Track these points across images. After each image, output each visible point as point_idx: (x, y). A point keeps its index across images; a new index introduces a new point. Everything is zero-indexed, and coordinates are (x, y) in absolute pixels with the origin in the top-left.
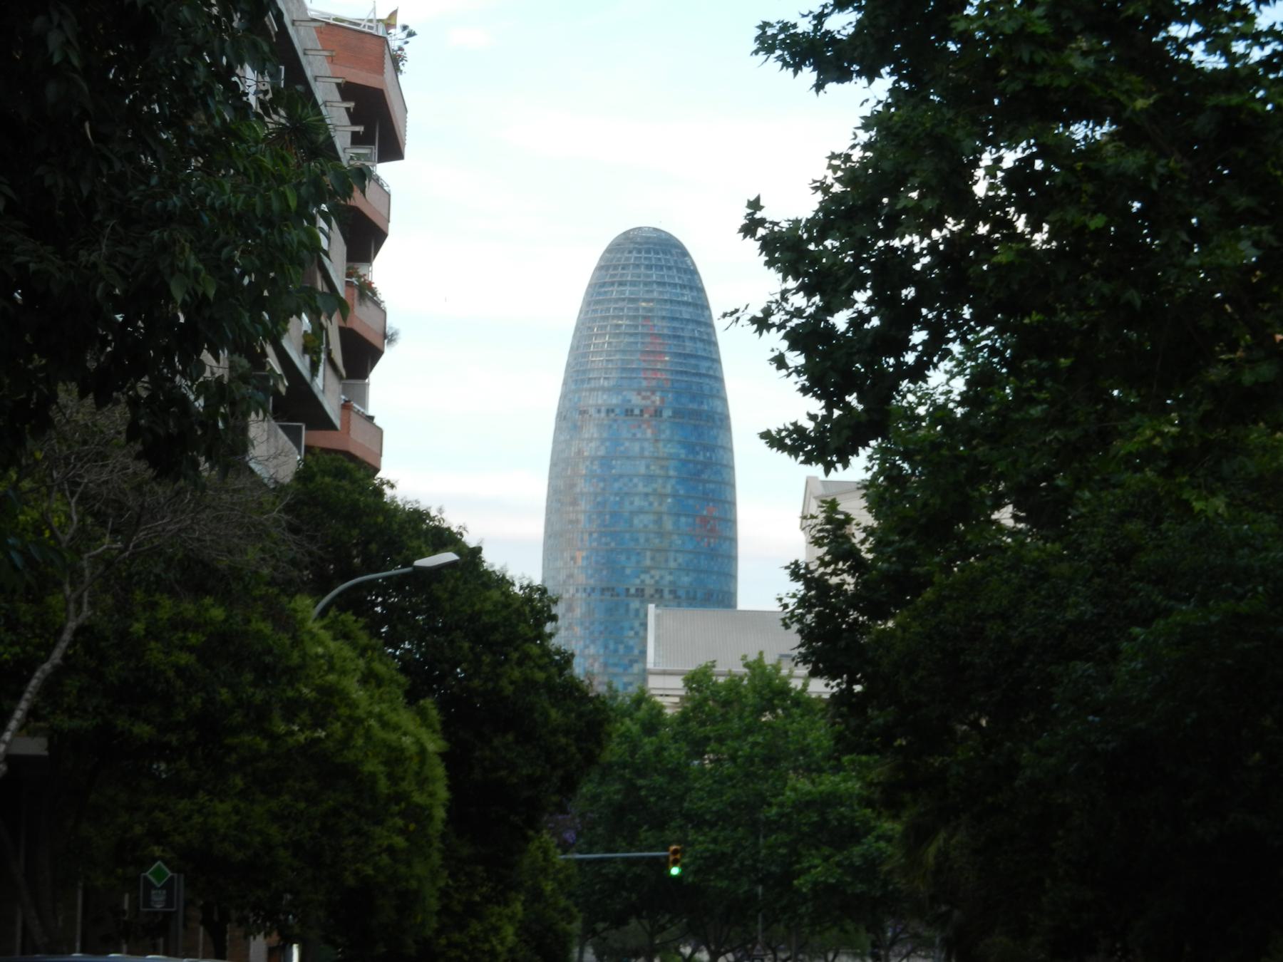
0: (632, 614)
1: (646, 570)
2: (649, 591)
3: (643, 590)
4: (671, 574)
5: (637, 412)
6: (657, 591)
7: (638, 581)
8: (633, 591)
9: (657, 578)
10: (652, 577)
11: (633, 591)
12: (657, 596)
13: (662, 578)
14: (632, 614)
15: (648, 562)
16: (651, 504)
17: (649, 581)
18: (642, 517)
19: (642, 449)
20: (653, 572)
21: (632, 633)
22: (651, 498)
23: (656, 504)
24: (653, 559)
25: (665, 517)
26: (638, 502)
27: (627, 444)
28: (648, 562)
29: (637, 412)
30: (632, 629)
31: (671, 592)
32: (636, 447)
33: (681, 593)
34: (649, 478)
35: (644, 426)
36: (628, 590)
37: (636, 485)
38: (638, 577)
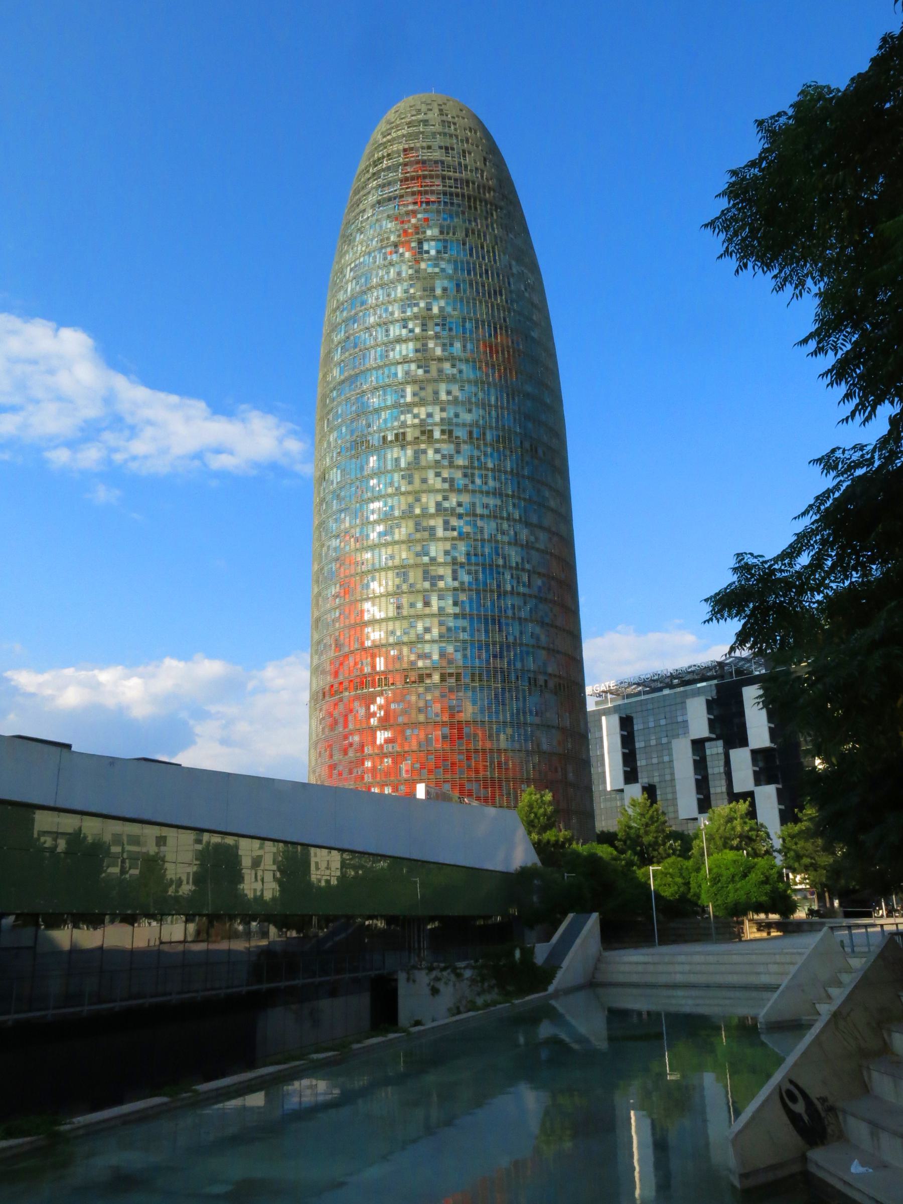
1: (408, 408)
3: (404, 434)
6: (423, 433)
9: (423, 416)
12: (424, 438)
13: (430, 415)
15: (409, 399)
16: (412, 331)
19: (399, 274)
20: (416, 411)
22: (410, 325)
23: (418, 330)
24: (414, 394)
28: (409, 399)
31: (443, 432)
34: (409, 301)
35: (401, 250)
36: (384, 438)
37: (392, 314)
38: (397, 418)
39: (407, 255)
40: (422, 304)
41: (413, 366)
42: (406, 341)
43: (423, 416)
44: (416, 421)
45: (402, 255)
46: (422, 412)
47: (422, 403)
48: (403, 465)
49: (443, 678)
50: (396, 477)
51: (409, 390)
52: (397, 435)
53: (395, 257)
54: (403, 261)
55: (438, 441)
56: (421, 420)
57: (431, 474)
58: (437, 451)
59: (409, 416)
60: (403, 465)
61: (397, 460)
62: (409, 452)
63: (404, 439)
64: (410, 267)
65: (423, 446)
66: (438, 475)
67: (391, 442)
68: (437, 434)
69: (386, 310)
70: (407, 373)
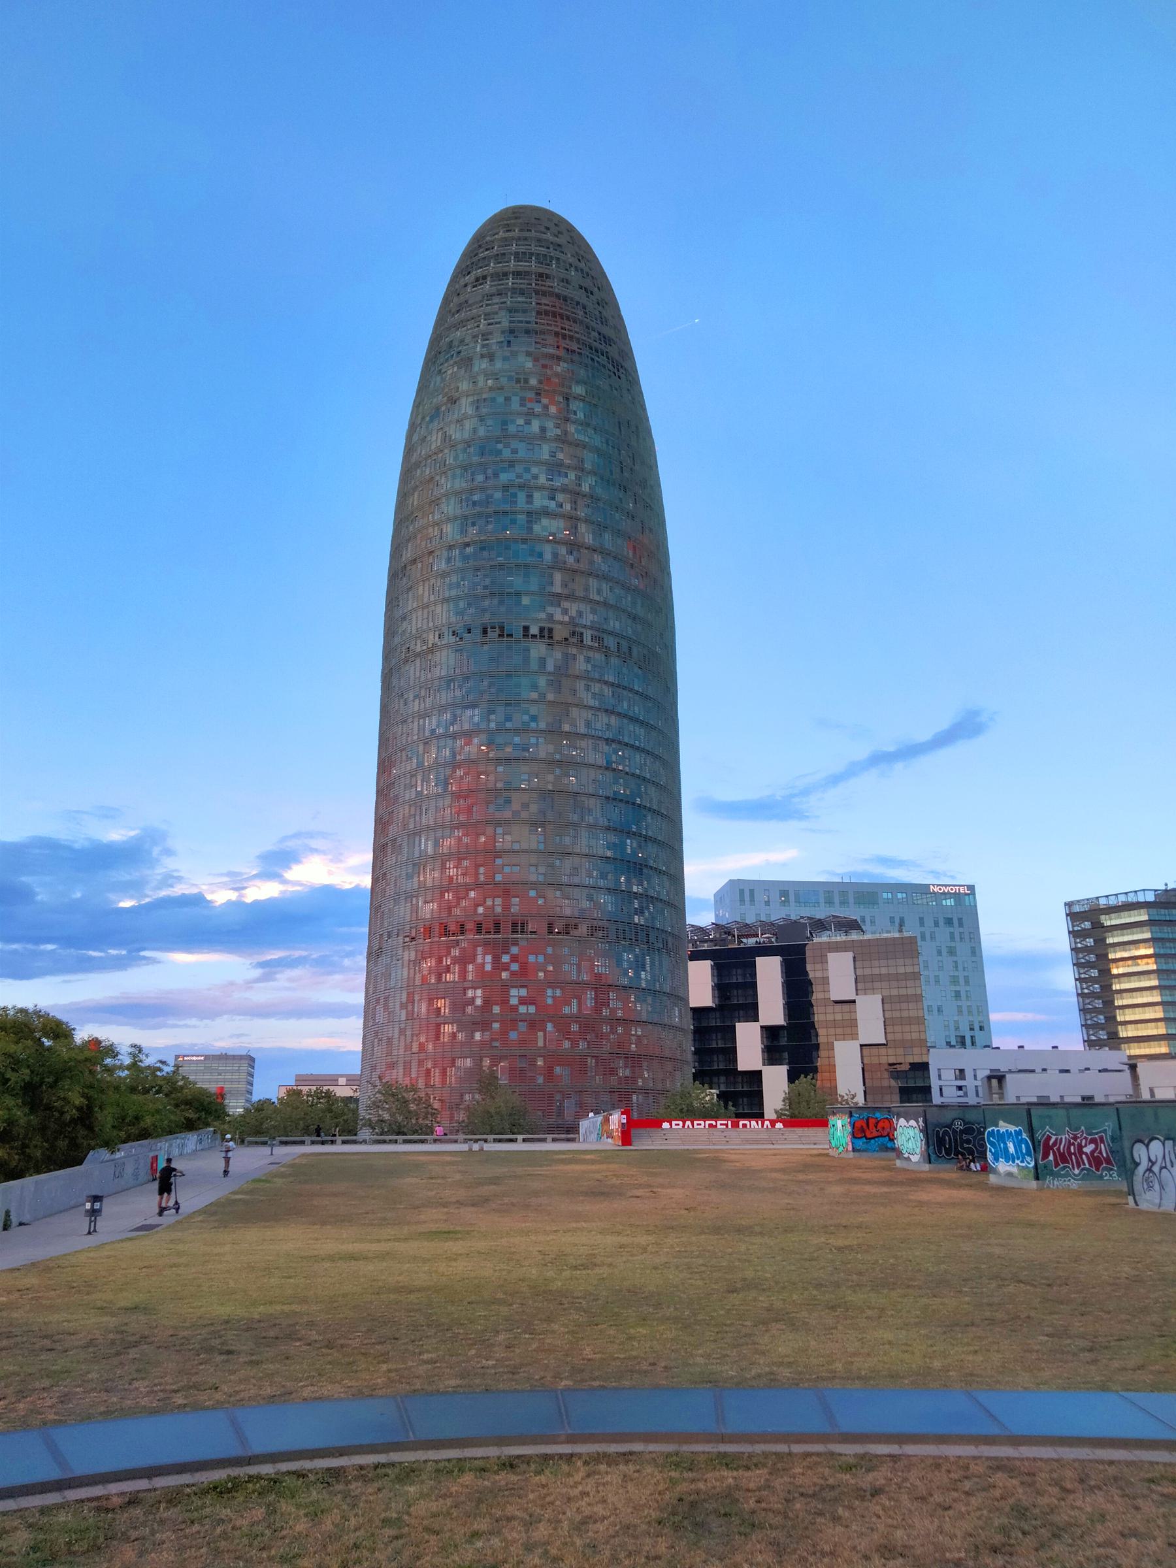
0: (534, 666)
2: (560, 633)
3: (551, 630)
4: (594, 612)
5: (533, 382)
6: (573, 633)
7: (542, 615)
8: (534, 630)
9: (574, 614)
10: (565, 612)
11: (534, 630)
12: (574, 640)
14: (534, 666)
17: (559, 617)
18: (545, 522)
19: (543, 429)
20: (566, 604)
21: (534, 695)
22: (560, 497)
23: (567, 507)
25: (582, 528)
26: (540, 500)
27: (521, 421)
28: (558, 588)
29: (533, 382)
30: (534, 687)
32: (535, 426)
33: (611, 642)
35: (545, 401)
36: (526, 629)
37: (536, 477)
38: (542, 608)
39: (553, 409)
40: (572, 475)
41: (563, 550)
42: (553, 515)
43: (574, 614)
44: (567, 619)
45: (546, 407)
46: (573, 608)
47: (572, 597)
48: (550, 667)
49: (593, 929)
50: (542, 682)
51: (558, 577)
52: (542, 629)
53: (538, 409)
54: (547, 415)
55: (590, 648)
56: (572, 618)
57: (580, 685)
58: (588, 660)
59: (559, 610)
60: (550, 667)
61: (542, 661)
62: (558, 655)
63: (551, 637)
64: (557, 426)
65: (574, 651)
66: (588, 688)
67: (534, 636)
68: (588, 640)
69: (527, 470)
70: (555, 555)
